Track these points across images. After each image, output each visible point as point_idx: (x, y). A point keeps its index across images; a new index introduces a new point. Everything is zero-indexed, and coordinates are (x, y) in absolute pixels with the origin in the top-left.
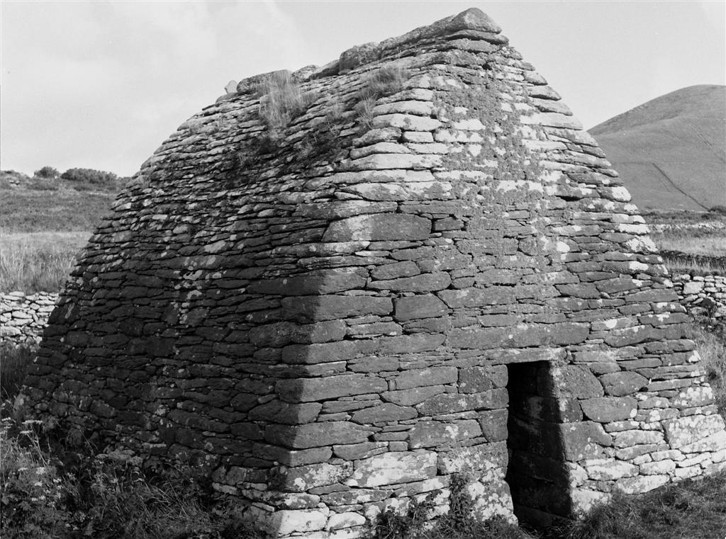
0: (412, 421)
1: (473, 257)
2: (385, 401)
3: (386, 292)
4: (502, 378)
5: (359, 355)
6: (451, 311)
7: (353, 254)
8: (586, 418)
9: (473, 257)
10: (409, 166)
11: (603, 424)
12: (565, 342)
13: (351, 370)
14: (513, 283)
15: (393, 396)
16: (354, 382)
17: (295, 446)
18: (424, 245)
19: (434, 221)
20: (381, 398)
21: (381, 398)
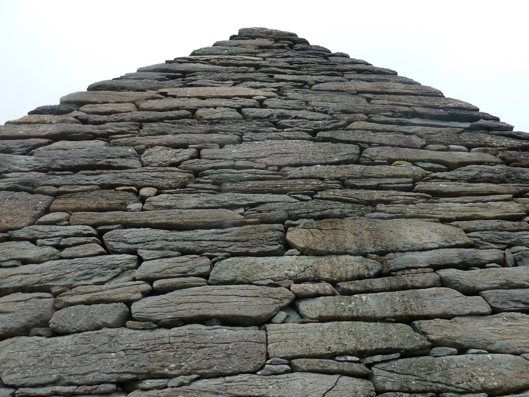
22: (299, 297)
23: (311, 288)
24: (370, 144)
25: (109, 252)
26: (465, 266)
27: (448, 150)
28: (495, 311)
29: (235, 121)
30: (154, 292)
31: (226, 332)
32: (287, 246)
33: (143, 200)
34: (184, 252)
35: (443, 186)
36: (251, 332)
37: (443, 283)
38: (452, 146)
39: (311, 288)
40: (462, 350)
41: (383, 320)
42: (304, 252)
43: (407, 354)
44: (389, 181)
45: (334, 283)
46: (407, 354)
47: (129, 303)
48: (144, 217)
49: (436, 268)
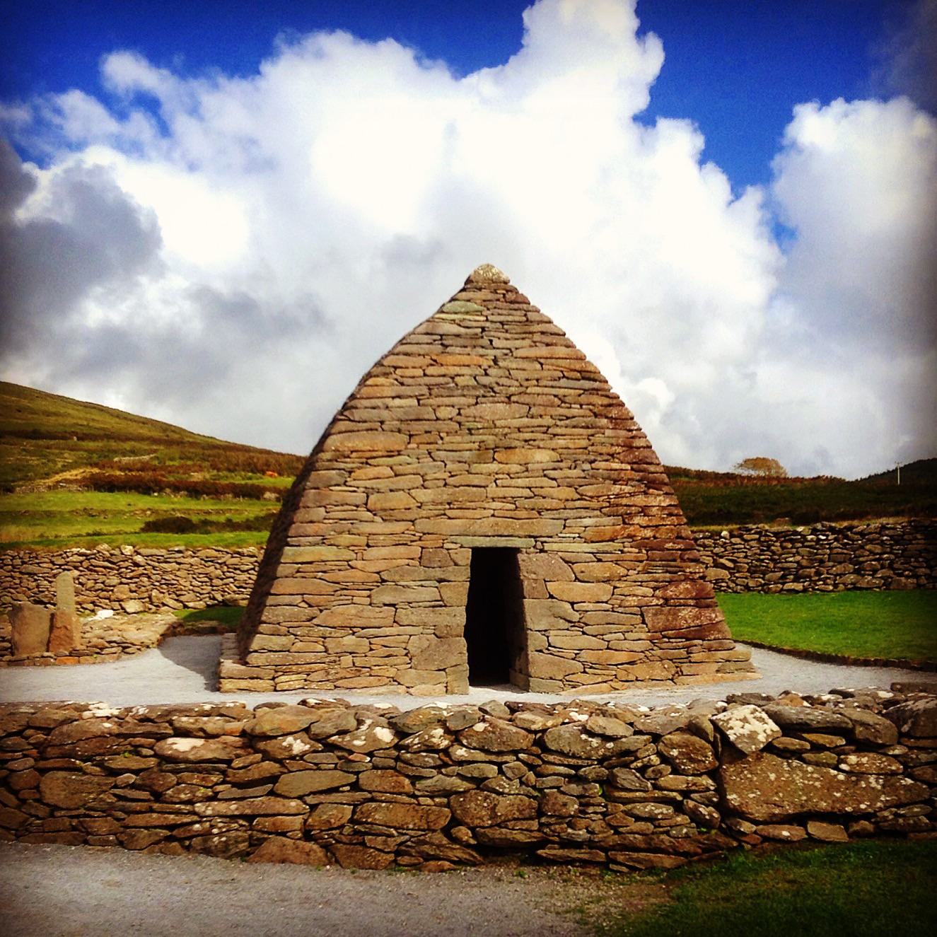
0: (375, 584)
1: (446, 465)
2: (352, 568)
3: (362, 489)
4: (465, 557)
5: (332, 533)
6: (419, 505)
7: (337, 461)
8: (551, 597)
9: (446, 465)
10: (394, 395)
11: (572, 604)
12: (535, 534)
13: (324, 543)
14: (483, 484)
15: (359, 564)
16: (326, 552)
17: (272, 591)
18: (399, 455)
19: (411, 436)
20: (349, 565)
21: (349, 565)
22: (497, 479)
23: (501, 476)
24: (534, 405)
25: (434, 460)
26: (554, 469)
27: (571, 407)
28: (559, 486)
29: (474, 388)
30: (452, 476)
31: (475, 489)
32: (494, 459)
33: (442, 438)
34: (460, 462)
35: (558, 431)
36: (483, 489)
37: (545, 476)
38: (573, 406)
39: (501, 476)
40: (544, 498)
41: (523, 488)
42: (499, 463)
43: (526, 498)
44: (538, 429)
45: (508, 474)
46: (526, 498)
47: (445, 480)
48: (445, 447)
49: (544, 470)
